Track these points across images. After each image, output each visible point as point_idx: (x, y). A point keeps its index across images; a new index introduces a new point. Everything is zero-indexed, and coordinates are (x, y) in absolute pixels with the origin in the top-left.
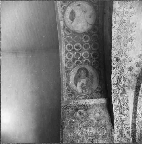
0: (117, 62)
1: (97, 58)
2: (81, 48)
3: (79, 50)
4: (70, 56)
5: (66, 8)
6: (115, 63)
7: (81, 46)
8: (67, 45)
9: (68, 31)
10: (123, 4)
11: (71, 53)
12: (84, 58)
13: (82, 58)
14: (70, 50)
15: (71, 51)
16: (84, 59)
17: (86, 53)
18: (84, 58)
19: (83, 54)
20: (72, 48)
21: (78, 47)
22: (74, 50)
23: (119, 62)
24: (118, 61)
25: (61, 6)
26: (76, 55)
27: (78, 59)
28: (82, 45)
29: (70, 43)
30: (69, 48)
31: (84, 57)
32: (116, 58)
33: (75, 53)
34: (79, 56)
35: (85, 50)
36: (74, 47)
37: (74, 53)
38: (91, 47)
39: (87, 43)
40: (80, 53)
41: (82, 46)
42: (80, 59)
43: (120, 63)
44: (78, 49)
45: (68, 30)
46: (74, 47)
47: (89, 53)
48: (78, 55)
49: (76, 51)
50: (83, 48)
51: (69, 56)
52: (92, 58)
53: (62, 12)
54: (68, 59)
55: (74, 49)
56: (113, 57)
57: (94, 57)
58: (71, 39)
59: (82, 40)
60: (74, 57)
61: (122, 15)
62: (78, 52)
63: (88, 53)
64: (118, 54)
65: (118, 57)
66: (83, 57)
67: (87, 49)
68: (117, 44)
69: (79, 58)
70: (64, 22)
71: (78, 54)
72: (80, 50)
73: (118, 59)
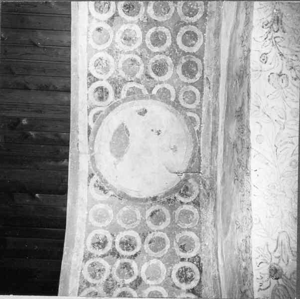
0: (274, 282)
1: (193, 284)
2: (137, 249)
3: (133, 253)
4: (98, 274)
5: (103, 117)
6: (266, 285)
7: (139, 240)
8: (92, 235)
9: (101, 188)
10: (284, 85)
11: (102, 261)
12: (149, 282)
13: (139, 281)
14: (101, 252)
15: (103, 256)
16: (148, 286)
17: (157, 266)
18: (149, 282)
19: (144, 268)
20: (109, 247)
21: (128, 244)
22: (114, 253)
23: (280, 281)
24: (277, 279)
25: (89, 111)
26: (118, 272)
27: (124, 286)
28: (144, 236)
29: (104, 228)
30: (99, 243)
31: (148, 278)
32: (269, 266)
33: (118, 262)
34: (131, 275)
35: (153, 254)
36: (114, 243)
37: (112, 263)
38: (172, 246)
39: (160, 231)
40: (134, 265)
41: (143, 242)
42: (131, 284)
43: (285, 287)
44: (128, 250)
45: (103, 185)
46: (114, 243)
47: (167, 266)
48: (125, 270)
49: (123, 256)
50: (146, 246)
51: (96, 272)
52: (174, 285)
53: (89, 127)
54: (90, 280)
55: (114, 249)
56: (259, 261)
57: (181, 282)
58: (108, 216)
59: (143, 221)
60: (111, 276)
61: (281, 120)
62: (126, 260)
63: (162, 266)
64: (275, 251)
65: (275, 261)
66: (144, 278)
67: (160, 254)
68: (269, 214)
69: (128, 281)
70: (93, 159)
71: (126, 266)
72: (136, 255)
73: (276, 271)
